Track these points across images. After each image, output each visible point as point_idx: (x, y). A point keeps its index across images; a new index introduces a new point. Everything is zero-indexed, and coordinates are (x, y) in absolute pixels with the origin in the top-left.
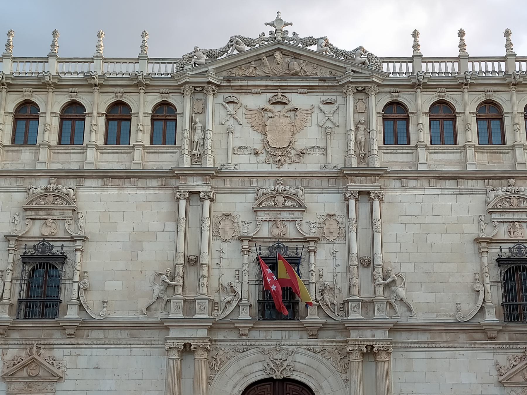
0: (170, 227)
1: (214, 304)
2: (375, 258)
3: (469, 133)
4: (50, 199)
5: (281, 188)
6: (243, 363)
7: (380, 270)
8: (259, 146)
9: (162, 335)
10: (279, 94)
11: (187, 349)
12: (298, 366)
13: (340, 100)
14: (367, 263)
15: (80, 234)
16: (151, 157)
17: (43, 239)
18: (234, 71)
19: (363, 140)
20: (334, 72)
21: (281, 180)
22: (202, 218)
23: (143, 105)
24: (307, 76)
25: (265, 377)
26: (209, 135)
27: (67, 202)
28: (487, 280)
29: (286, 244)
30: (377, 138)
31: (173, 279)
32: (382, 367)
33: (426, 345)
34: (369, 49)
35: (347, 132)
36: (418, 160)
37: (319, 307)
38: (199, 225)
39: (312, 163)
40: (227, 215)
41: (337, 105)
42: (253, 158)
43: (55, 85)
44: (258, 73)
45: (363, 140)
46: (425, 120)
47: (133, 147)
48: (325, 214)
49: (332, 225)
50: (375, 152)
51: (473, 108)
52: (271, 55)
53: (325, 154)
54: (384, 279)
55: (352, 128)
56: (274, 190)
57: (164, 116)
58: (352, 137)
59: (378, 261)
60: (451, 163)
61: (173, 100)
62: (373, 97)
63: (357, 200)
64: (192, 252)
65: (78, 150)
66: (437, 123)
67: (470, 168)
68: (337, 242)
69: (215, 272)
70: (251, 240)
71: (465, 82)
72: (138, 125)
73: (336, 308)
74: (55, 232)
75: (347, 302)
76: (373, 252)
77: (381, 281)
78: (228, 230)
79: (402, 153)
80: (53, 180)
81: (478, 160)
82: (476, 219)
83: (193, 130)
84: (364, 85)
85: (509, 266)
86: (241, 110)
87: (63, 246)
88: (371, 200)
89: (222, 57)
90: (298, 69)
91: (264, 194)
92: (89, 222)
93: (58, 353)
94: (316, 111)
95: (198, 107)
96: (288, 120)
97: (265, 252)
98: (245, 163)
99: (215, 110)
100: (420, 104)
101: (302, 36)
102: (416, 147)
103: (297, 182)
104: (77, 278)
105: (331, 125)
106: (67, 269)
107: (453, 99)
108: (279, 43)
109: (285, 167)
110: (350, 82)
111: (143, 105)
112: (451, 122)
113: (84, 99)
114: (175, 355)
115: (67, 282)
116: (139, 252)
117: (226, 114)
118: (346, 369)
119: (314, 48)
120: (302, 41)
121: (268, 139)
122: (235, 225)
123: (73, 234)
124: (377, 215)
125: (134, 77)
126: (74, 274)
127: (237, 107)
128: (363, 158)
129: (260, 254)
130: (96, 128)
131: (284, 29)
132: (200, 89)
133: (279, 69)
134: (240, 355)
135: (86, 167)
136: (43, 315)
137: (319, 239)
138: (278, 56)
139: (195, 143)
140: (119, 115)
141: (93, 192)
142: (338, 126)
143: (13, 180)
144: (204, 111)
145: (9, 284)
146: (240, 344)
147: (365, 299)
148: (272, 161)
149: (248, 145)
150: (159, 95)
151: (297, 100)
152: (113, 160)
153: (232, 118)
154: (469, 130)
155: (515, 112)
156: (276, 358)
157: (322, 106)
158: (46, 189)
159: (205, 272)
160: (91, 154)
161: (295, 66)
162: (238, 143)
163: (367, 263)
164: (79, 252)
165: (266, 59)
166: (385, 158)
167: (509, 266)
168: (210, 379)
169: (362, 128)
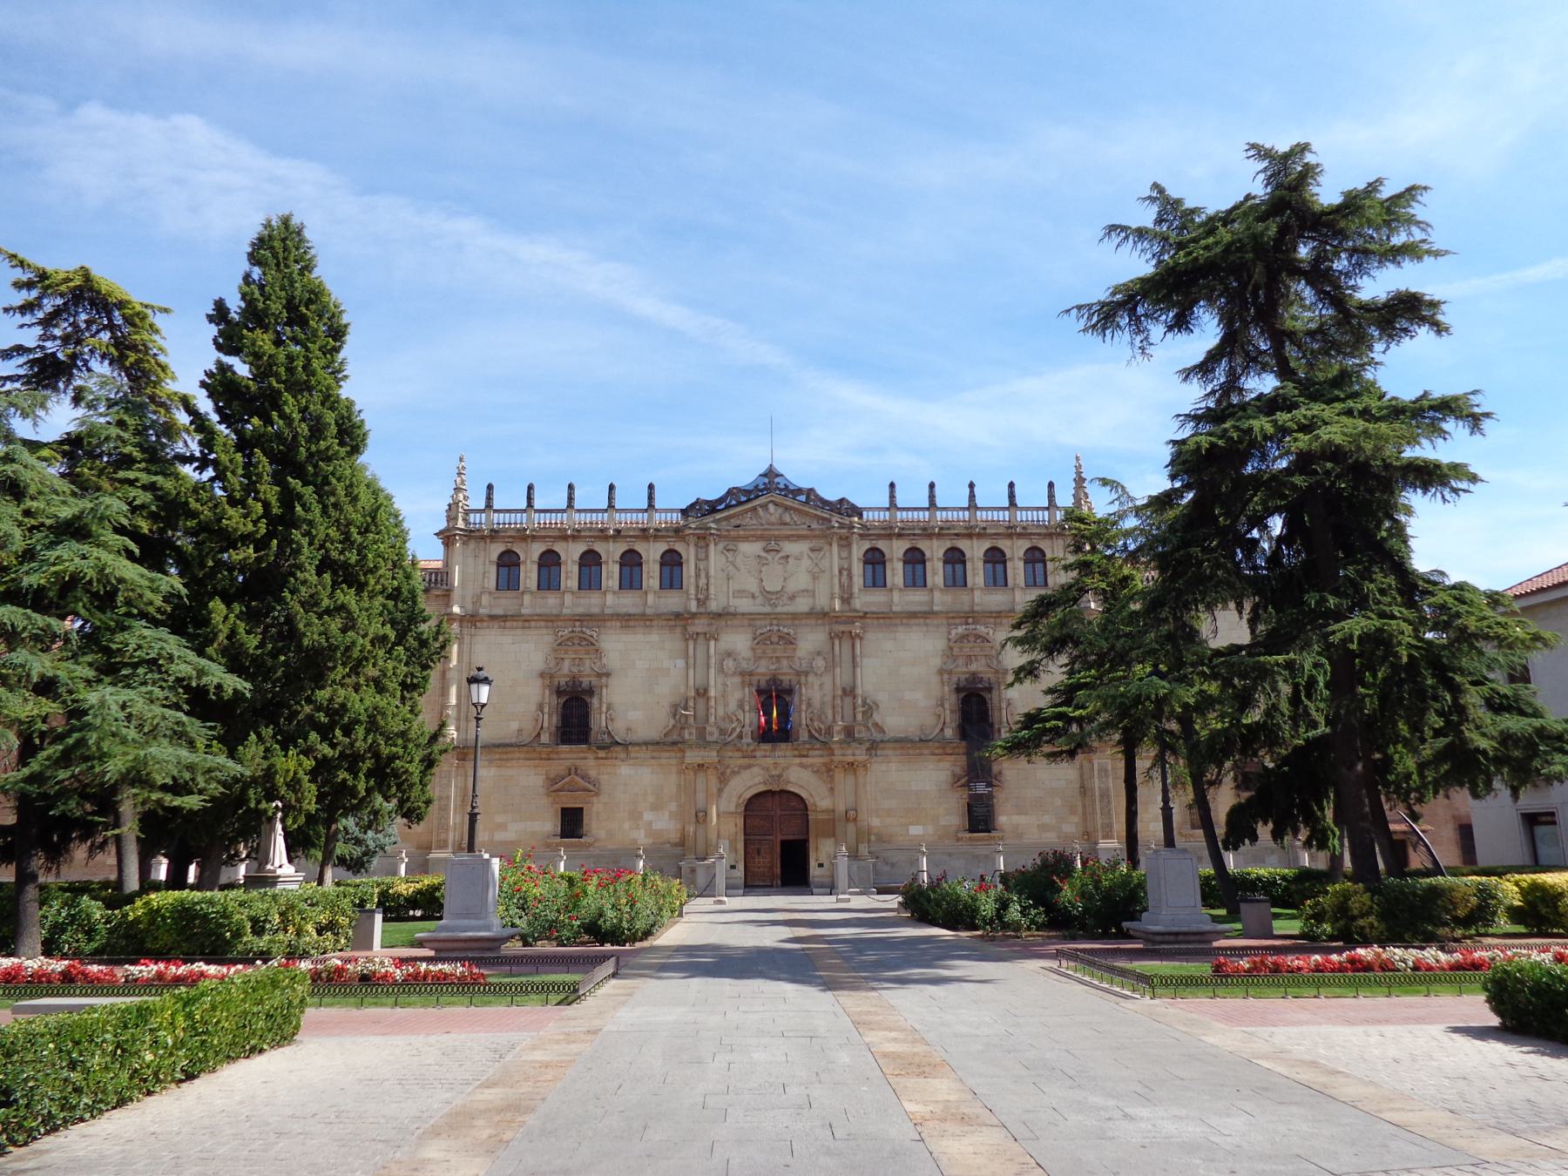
0: (681, 663)
13: (826, 547)
22: (708, 657)
23: (652, 553)
26: (712, 581)
28: (947, 706)
30: (858, 581)
34: (852, 500)
35: (832, 577)
39: (802, 605)
43: (577, 535)
46: (900, 566)
51: (941, 554)
52: (764, 506)
57: (671, 561)
58: (836, 581)
59: (859, 691)
61: (679, 547)
66: (909, 567)
70: (751, 674)
81: (942, 600)
83: (697, 576)
88: (853, 638)
93: (593, 773)
98: (744, 605)
100: (896, 550)
106: (595, 701)
109: (779, 609)
111: (652, 553)
113: (599, 547)
119: (803, 498)
120: (792, 492)
130: (611, 573)
132: (703, 539)
133: (773, 519)
135: (607, 611)
136: (580, 742)
140: (631, 561)
144: (707, 558)
151: (790, 548)
154: (936, 572)
159: (712, 703)
160: (610, 599)
161: (787, 518)
166: (866, 600)
168: (720, 791)
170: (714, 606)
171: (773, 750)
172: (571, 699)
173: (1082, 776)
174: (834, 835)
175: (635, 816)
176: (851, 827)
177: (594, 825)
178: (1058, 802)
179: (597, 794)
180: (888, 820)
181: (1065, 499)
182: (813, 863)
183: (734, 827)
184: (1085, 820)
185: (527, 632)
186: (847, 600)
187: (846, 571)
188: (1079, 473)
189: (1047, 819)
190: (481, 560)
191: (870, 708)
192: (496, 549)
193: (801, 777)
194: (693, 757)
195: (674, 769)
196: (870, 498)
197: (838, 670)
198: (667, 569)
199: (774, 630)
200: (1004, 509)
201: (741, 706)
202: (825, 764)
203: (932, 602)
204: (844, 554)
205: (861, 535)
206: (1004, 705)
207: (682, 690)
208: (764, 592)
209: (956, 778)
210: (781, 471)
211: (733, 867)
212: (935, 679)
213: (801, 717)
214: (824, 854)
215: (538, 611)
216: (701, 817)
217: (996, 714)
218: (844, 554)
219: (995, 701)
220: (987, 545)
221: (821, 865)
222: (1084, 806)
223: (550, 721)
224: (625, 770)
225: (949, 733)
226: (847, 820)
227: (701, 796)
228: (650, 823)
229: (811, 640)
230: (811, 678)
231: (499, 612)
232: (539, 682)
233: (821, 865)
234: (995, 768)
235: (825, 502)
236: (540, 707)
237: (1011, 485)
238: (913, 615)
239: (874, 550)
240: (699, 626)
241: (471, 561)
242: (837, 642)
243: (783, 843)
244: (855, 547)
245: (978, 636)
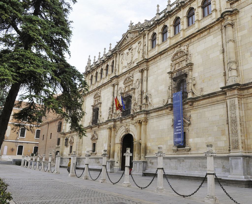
178: (216, 129)
189: (211, 140)
234: (188, 114)
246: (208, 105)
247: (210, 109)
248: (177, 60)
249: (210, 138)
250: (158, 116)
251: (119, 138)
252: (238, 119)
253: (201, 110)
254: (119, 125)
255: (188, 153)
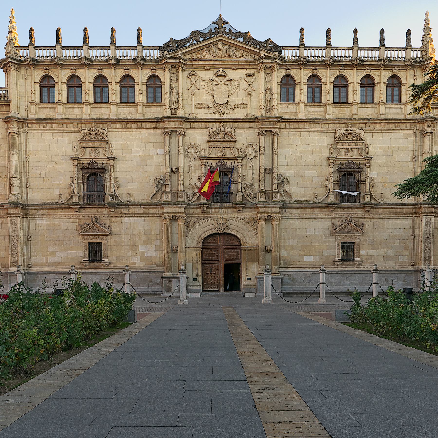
0: (161, 152)
1: (188, 196)
2: (274, 169)
3: (328, 95)
4: (93, 136)
5: (222, 128)
6: (203, 225)
7: (276, 175)
8: (210, 104)
9: (161, 211)
10: (221, 70)
11: (174, 218)
12: (232, 226)
13: (256, 74)
14: (269, 171)
15: (112, 156)
16: (148, 109)
17: (92, 159)
18: (194, 54)
19: (269, 99)
20: (253, 55)
21: (222, 124)
23: (141, 76)
24: (237, 58)
25: (215, 232)
26: (180, 96)
27: (103, 138)
28: (331, 181)
29: (225, 161)
30: (277, 98)
31: (164, 181)
32: (275, 226)
33: (298, 215)
36: (299, 111)
37: (243, 195)
38: (177, 151)
39: (240, 114)
40: (192, 145)
41: (254, 77)
42: (206, 109)
44: (209, 56)
45: (269, 99)
46: (305, 87)
47: (137, 104)
48: (247, 144)
49: (251, 151)
50: (275, 106)
52: (216, 44)
53: (248, 108)
54: (278, 181)
55: (263, 92)
56: (219, 130)
57: (154, 83)
58: (263, 97)
59: (275, 170)
60: (317, 113)
61: (159, 73)
62: (276, 72)
63: (265, 135)
64: (174, 166)
65: (106, 106)
67: (328, 116)
68: (253, 160)
69: (187, 177)
70: (206, 158)
71: (328, 63)
72: (139, 90)
73: (252, 196)
74: (98, 155)
75: (258, 193)
76: (273, 165)
77: (276, 182)
78: (193, 153)
79: (291, 107)
80: (94, 125)
81: (332, 112)
82: (329, 146)
83: (171, 93)
84: (271, 64)
85: (344, 173)
86: (199, 80)
87: (103, 163)
88: (273, 136)
89: (187, 45)
90: (232, 54)
91: (213, 132)
92: (117, 150)
93: (107, 221)
94: (242, 80)
95: (174, 79)
96: (226, 87)
97: (214, 166)
98: (202, 113)
99: (183, 80)
101: (234, 31)
102: (299, 103)
103: (231, 125)
104: (112, 181)
105: (251, 90)
107: (321, 73)
108: (221, 36)
109: (225, 116)
110: (263, 62)
111: (141, 76)
112: (319, 89)
114: (168, 221)
115: (107, 183)
116: (145, 167)
117: (190, 82)
118: (257, 228)
119: (241, 39)
121: (215, 99)
122: (197, 150)
123: (108, 156)
124: (276, 145)
125: (80, 59)
126: (111, 179)
127: (196, 79)
128: (269, 110)
129: (211, 167)
130: (114, 92)
131: (224, 26)
133: (221, 53)
134: (201, 221)
137: (243, 158)
138: (220, 44)
139: (173, 101)
141: (117, 132)
142: (255, 91)
143: (71, 125)
144: (177, 81)
145: (77, 184)
146: (203, 215)
147: (267, 191)
148: (217, 112)
149: (203, 103)
150: (150, 71)
151: (232, 74)
152: (126, 112)
153: (193, 85)
155: (355, 83)
156: (220, 222)
157: (245, 78)
158: (90, 130)
159: (181, 177)
161: (230, 51)
162: (197, 102)
163: (269, 171)
164: (112, 167)
165: (213, 47)
167: (344, 173)
168: (187, 233)
169: (269, 91)
170: (181, 113)
171: (221, 208)
172: (91, 175)
173: (413, 226)
174: (258, 261)
175: (134, 248)
176: (268, 256)
177: (109, 253)
178: (397, 242)
179: (110, 234)
180: (292, 252)
181: (417, 42)
182: (244, 278)
183: (195, 255)
184: (413, 254)
185: (62, 131)
186: (269, 110)
187: (268, 90)
188: (426, 24)
189: (390, 253)
190: (29, 81)
191: (282, 182)
192: (39, 74)
193: (238, 226)
194: (169, 211)
195: (158, 220)
196: (286, 39)
197: (262, 156)
198: (151, 90)
199: (222, 130)
200: (375, 49)
201: (199, 179)
202: (253, 217)
203: (325, 113)
204: (268, 79)
205: (280, 65)
206: (367, 181)
207: (162, 169)
208: (215, 103)
209: (334, 227)
210: (227, 21)
211: (195, 280)
212: (325, 163)
213: (238, 187)
214: (250, 272)
215: (67, 116)
216: (174, 251)
217: (363, 186)
218: (268, 79)
219: (363, 179)
220: (363, 73)
221: (249, 279)
222: (413, 246)
223: (79, 189)
224: (127, 221)
225: (332, 198)
226: (266, 251)
227: (175, 236)
228: (144, 253)
229: (245, 137)
230: (245, 162)
231: (42, 116)
232: (71, 163)
233: (249, 279)
235: (255, 42)
236: (72, 179)
237: (382, 32)
238: (313, 121)
239: (288, 76)
240: (173, 125)
241: (22, 82)
242: (262, 137)
243: (226, 265)
244: (275, 73)
245: (354, 135)
246: (392, 215)
247: (392, 220)
248: (345, 144)
249: (389, 251)
250: (301, 216)
251: (196, 238)
252: (432, 237)
253: (380, 220)
254: (198, 215)
255: (358, 266)
